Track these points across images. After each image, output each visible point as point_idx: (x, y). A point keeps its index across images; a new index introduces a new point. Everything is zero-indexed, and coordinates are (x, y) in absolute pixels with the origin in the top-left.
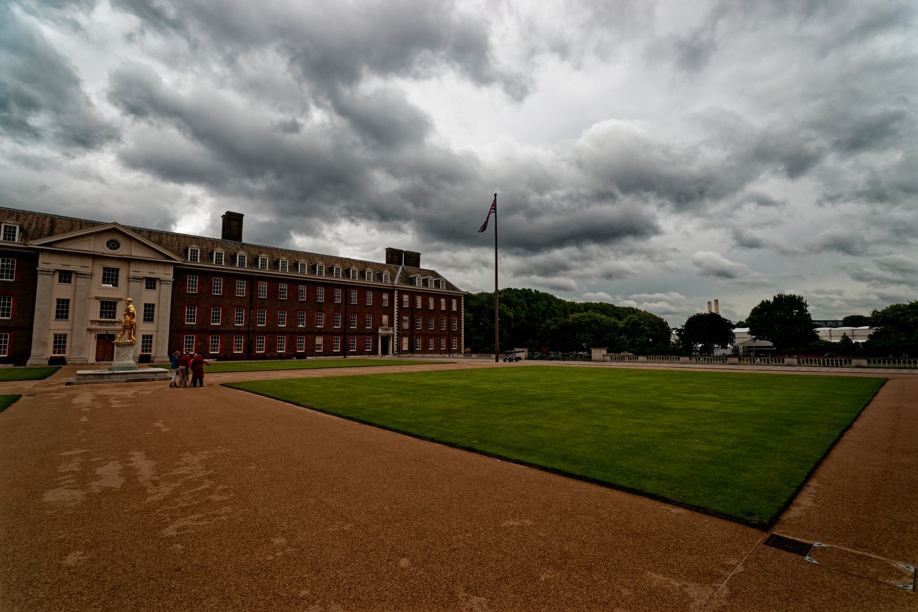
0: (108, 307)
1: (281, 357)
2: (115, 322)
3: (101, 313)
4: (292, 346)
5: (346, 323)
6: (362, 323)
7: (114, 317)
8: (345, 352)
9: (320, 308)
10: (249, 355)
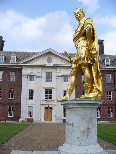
3: (46, 95)
7: (51, 98)
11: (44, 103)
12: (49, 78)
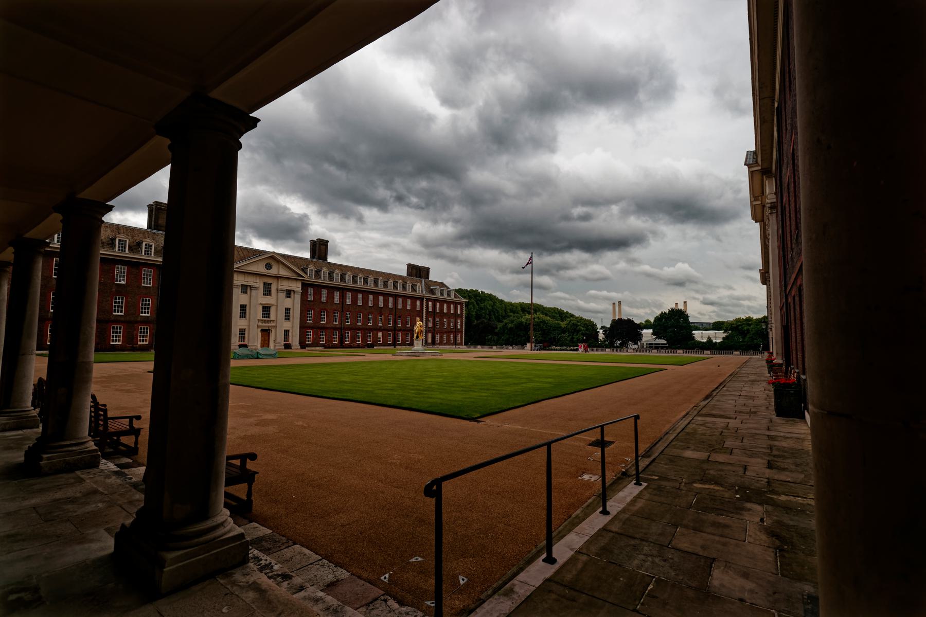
0: (266, 310)
1: (358, 346)
2: (270, 321)
4: (365, 339)
5: (395, 322)
6: (404, 324)
8: (394, 344)
9: (381, 311)
10: (341, 345)
11: (260, 324)
12: (267, 291)
